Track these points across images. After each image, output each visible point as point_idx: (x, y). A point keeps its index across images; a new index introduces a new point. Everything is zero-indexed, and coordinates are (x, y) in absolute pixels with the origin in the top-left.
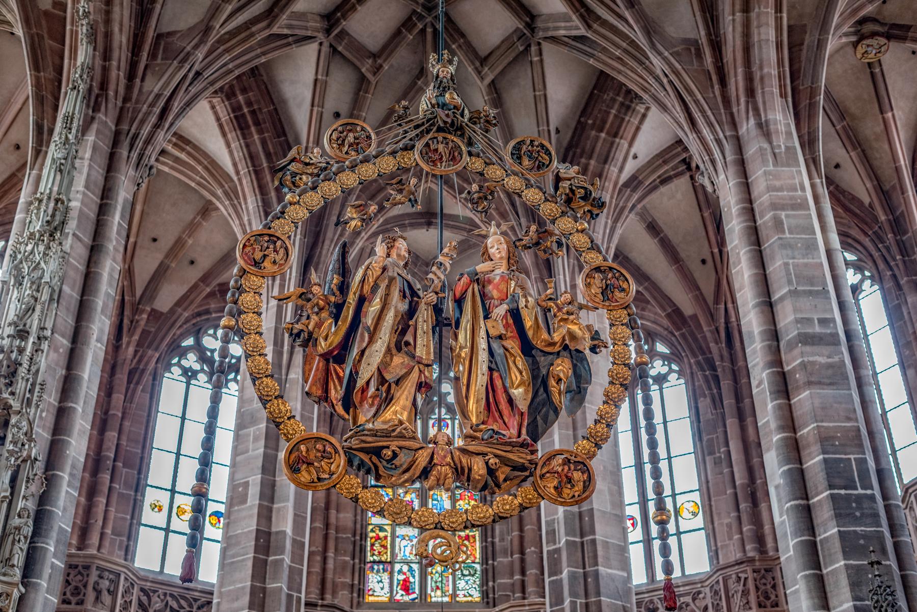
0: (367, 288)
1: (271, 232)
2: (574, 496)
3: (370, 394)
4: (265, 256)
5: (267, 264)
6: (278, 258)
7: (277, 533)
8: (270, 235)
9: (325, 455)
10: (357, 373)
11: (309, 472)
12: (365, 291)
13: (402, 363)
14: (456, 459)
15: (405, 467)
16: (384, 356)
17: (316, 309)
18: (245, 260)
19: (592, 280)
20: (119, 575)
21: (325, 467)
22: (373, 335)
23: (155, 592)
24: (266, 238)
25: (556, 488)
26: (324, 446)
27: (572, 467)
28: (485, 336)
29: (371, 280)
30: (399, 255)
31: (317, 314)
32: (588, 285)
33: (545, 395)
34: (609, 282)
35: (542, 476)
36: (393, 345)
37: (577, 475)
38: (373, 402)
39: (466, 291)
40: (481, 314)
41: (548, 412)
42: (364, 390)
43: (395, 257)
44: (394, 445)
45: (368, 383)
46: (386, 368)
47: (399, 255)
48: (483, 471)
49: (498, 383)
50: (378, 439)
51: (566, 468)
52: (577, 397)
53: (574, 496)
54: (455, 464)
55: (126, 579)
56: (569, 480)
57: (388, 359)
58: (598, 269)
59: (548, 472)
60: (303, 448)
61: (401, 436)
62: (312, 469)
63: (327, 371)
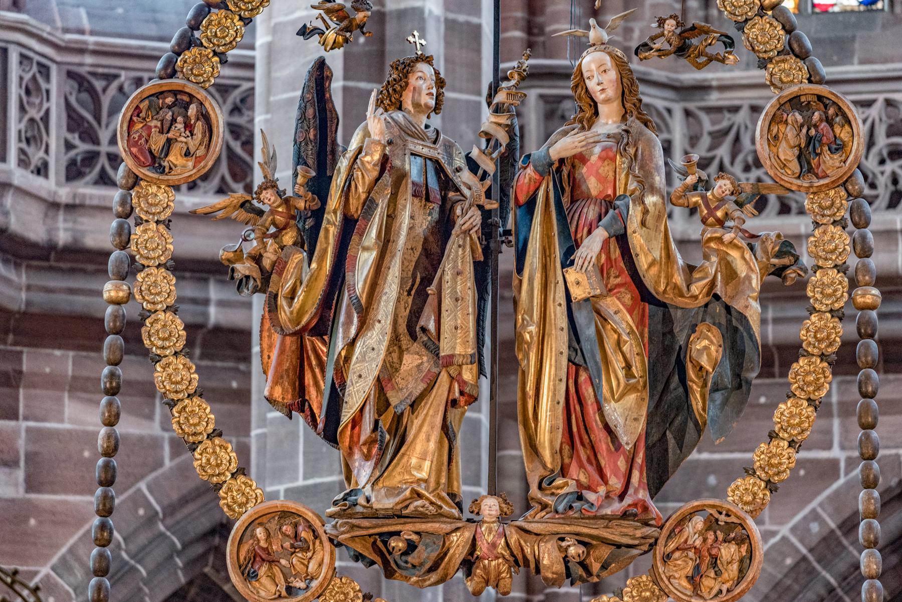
0: (355, 205)
1: (177, 82)
2: (720, 591)
3: (363, 438)
4: (169, 142)
5: (175, 158)
6: (193, 144)
7: (402, 14)
8: (175, 93)
9: (299, 546)
10: (343, 385)
11: (273, 578)
12: (352, 209)
13: (418, 366)
14: (512, 541)
15: (427, 566)
16: (389, 352)
17: (272, 230)
18: (135, 157)
19: (782, 127)
20: (5, 51)
21: (299, 567)
22: (365, 313)
23: (110, 78)
24: (169, 100)
25: (690, 579)
26: (296, 526)
27: (721, 536)
28: (563, 302)
29: (360, 189)
30: (417, 105)
31: (274, 236)
32: (774, 140)
33: (681, 390)
34: (813, 132)
35: (667, 558)
36: (403, 328)
37: (728, 552)
38: (369, 451)
39: (537, 189)
40: (558, 254)
41: (685, 423)
42: (356, 422)
43: (411, 108)
44: (408, 530)
45: (362, 409)
46: (390, 380)
47: (417, 105)
48: (560, 567)
49: (588, 392)
50: (379, 521)
51: (711, 536)
52: (735, 397)
53: (720, 591)
54: (512, 554)
55: (24, 59)
56: (714, 561)
57: (395, 356)
58: (795, 102)
59: (677, 549)
60: (260, 532)
61: (420, 516)
62: (276, 570)
63: (302, 348)
